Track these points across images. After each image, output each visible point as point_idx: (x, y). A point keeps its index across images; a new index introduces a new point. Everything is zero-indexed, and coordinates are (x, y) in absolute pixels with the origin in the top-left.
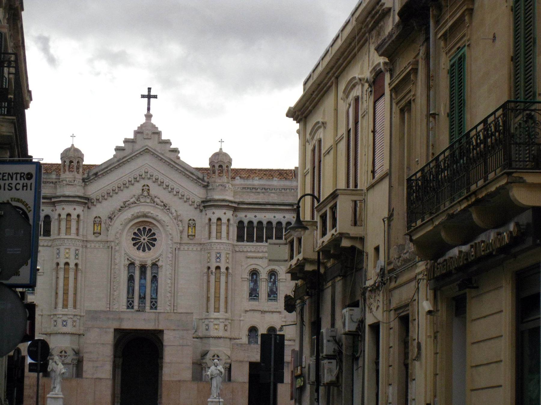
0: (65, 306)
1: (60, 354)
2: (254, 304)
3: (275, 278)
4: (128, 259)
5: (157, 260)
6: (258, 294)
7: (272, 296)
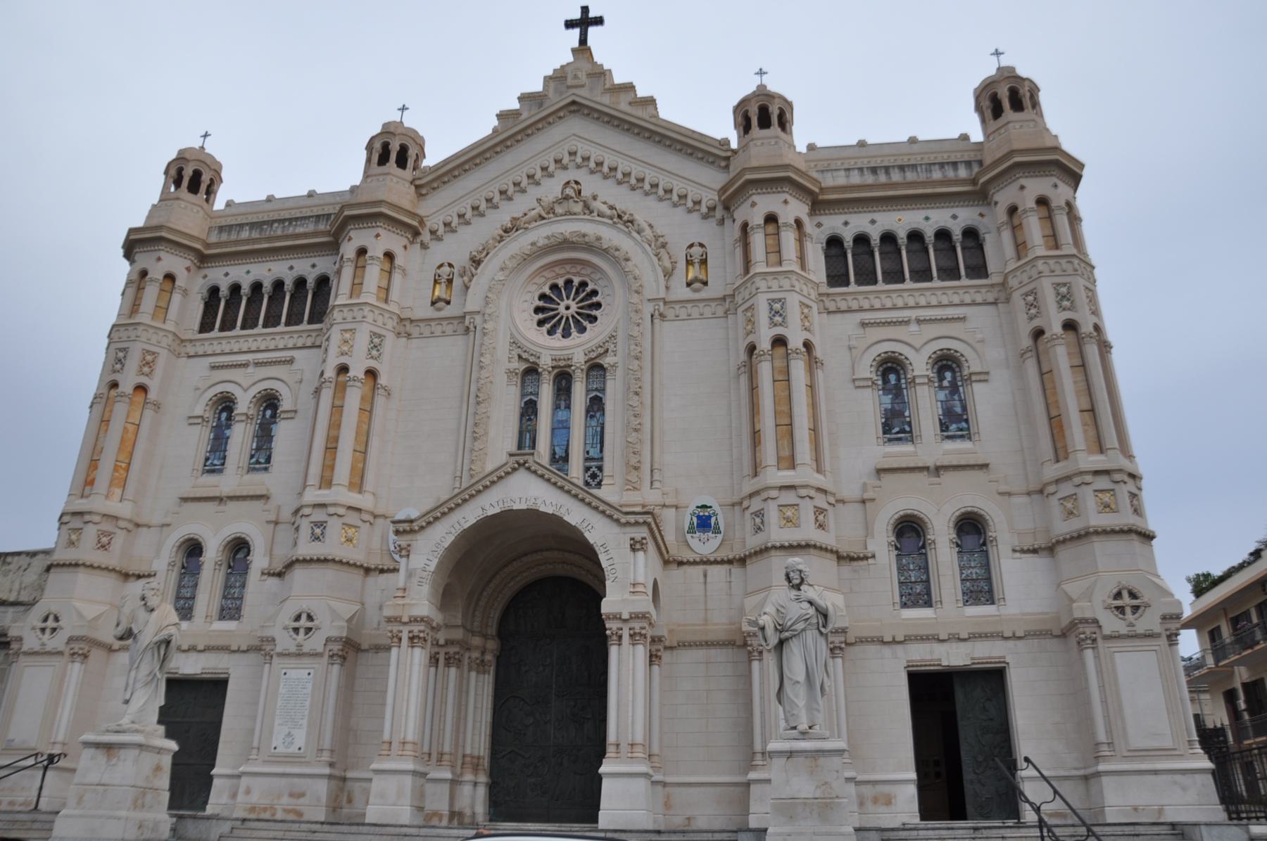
0: (326, 482)
1: (296, 625)
2: (901, 452)
3: (954, 378)
4: (520, 357)
5: (601, 350)
6: (910, 424)
7: (953, 427)
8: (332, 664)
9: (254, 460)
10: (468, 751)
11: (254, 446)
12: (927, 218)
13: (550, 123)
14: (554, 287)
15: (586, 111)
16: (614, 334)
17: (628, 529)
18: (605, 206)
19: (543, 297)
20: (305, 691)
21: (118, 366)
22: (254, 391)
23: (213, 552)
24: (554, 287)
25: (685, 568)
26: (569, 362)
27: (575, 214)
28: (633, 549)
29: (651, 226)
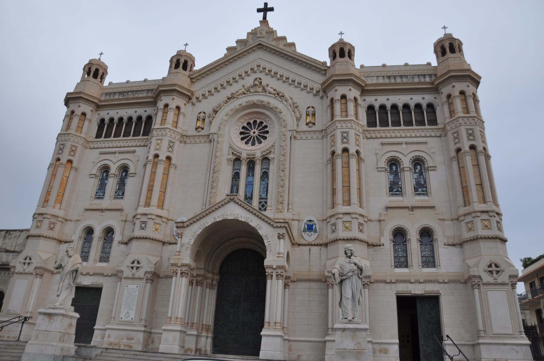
0: (148, 204)
1: (132, 265)
2: (397, 200)
3: (421, 168)
4: (233, 153)
5: (268, 152)
6: (401, 188)
7: (420, 190)
8: (147, 283)
9: (117, 194)
10: (204, 323)
11: (117, 188)
12: (411, 99)
13: (249, 53)
14: (249, 124)
15: (265, 48)
16: (274, 145)
17: (277, 229)
18: (272, 89)
19: (244, 128)
20: (135, 294)
21: (60, 152)
22: (118, 164)
23: (98, 233)
24: (249, 124)
25: (301, 247)
26: (254, 156)
27: (259, 92)
28: (279, 238)
29: (291, 98)
